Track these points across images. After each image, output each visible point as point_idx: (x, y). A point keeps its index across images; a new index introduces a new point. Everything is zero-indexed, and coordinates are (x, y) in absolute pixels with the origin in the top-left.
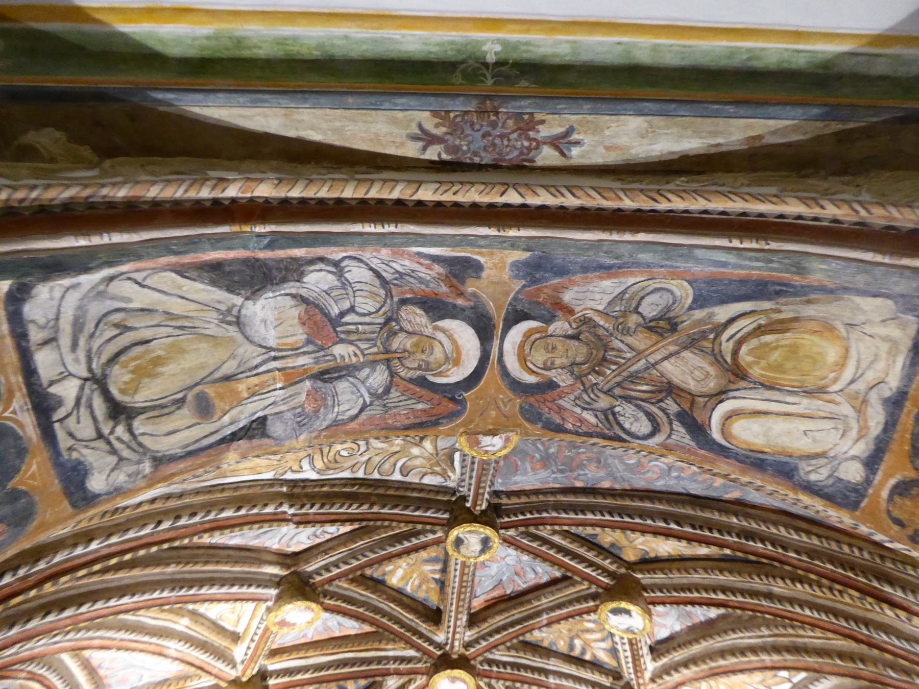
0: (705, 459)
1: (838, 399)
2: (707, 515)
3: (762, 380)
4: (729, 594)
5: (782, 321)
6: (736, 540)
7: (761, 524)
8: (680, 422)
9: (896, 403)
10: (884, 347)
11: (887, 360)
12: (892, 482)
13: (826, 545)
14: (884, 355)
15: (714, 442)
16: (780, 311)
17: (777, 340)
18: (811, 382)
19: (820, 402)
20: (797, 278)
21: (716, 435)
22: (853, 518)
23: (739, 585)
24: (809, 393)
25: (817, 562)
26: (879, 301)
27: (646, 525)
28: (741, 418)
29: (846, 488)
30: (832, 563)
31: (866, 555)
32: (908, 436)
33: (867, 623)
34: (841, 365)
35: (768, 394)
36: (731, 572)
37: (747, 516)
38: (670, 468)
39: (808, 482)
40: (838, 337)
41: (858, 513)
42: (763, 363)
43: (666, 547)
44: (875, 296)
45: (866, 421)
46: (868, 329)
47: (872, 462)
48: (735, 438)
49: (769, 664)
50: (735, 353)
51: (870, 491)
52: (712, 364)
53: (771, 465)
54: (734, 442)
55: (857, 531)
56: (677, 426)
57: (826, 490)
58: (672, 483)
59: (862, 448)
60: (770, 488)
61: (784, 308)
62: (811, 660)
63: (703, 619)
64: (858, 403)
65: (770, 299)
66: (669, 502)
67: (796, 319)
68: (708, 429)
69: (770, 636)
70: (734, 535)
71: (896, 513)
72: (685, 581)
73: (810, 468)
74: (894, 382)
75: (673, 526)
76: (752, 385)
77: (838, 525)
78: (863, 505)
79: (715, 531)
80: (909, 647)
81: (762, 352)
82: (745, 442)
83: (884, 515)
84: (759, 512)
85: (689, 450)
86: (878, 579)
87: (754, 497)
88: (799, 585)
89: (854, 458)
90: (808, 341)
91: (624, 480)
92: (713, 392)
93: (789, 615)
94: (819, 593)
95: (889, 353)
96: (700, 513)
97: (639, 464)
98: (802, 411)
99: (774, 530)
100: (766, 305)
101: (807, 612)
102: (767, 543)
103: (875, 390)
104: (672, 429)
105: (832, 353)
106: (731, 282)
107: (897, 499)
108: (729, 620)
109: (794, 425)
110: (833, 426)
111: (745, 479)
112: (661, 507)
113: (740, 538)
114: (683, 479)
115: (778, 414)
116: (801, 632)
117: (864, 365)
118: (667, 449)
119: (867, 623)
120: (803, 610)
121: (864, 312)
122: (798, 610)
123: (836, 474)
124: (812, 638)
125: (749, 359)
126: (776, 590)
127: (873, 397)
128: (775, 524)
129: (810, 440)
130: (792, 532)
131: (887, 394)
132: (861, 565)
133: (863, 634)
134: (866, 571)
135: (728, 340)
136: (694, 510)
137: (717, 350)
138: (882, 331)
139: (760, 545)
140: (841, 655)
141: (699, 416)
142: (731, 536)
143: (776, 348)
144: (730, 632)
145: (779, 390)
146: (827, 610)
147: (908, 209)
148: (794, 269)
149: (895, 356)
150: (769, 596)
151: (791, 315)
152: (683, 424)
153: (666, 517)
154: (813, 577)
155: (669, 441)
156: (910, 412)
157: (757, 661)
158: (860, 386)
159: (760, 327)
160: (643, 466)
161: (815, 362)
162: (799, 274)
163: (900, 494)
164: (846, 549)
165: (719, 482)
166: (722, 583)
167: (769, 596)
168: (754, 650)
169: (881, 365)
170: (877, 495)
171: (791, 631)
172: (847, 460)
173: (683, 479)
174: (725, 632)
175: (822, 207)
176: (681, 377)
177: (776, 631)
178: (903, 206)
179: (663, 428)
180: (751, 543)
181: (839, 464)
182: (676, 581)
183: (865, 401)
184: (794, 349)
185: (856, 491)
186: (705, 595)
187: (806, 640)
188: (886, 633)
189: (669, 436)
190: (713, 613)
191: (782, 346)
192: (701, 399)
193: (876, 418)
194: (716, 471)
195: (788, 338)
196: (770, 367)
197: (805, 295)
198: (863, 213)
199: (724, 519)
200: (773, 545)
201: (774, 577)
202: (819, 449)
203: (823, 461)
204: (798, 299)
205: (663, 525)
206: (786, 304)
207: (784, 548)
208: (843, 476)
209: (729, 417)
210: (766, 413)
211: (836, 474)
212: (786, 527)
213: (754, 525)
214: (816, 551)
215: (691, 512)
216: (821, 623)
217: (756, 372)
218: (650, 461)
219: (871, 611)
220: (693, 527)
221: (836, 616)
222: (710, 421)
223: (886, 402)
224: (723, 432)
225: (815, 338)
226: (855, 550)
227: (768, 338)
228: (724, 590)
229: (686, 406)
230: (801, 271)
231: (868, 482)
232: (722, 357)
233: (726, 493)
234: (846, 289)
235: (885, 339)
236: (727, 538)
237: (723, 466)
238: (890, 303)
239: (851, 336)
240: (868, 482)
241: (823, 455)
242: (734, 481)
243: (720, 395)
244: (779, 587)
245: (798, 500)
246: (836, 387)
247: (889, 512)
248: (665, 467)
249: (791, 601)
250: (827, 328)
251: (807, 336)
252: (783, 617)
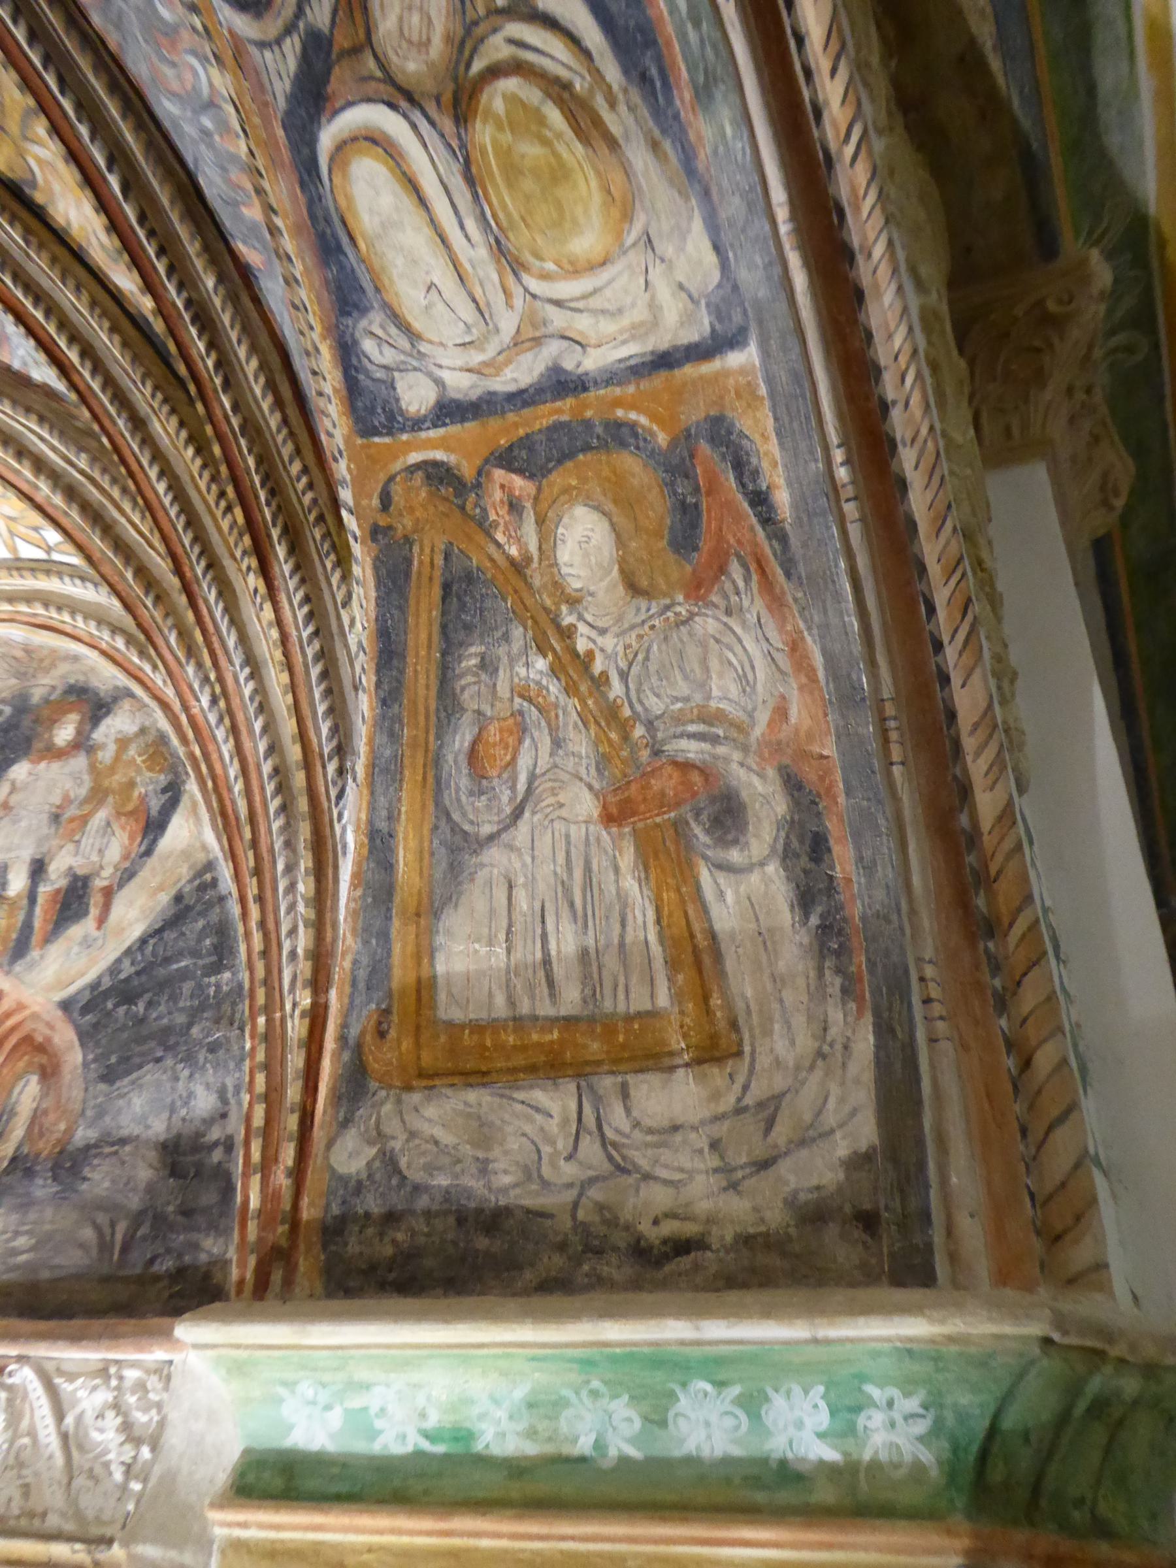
0: (269, 144)
1: (518, 302)
2: (183, 231)
3: (476, 155)
4: (88, 364)
5: (597, 122)
6: (180, 304)
7: (238, 327)
8: (304, 49)
9: (561, 384)
10: (639, 314)
11: (621, 332)
12: (439, 455)
13: (280, 439)
14: (626, 321)
15: (311, 143)
16: (612, 105)
17: (559, 135)
18: (519, 241)
19: (495, 276)
20: (687, 95)
21: (327, 137)
22: (347, 441)
23: (116, 371)
24: (500, 250)
25: (243, 442)
26: (711, 258)
27: (72, 126)
28: (386, 164)
29: (385, 402)
30: (259, 462)
31: (307, 498)
32: (521, 432)
33: (213, 565)
34: (575, 269)
35: (457, 183)
36: (125, 344)
37: (233, 298)
38: (211, 105)
39: (356, 343)
40: (619, 236)
41: (359, 441)
42: (507, 138)
43: (75, 211)
44: (717, 248)
45: (508, 362)
46: (656, 273)
47: (449, 411)
48: (345, 175)
49: (39, 498)
50: (495, 72)
51: (405, 437)
52: (448, 39)
53: (342, 268)
54: (337, 180)
55: (334, 465)
56: (292, 46)
57: (361, 377)
58: (189, 129)
59: (461, 384)
60: (303, 294)
61: (622, 108)
62: (97, 542)
63: (16, 365)
64: (529, 333)
65: (626, 72)
66: (150, 146)
67: (612, 143)
68: (327, 113)
69: (82, 472)
70: (185, 294)
71: (397, 490)
72: (45, 283)
73: (380, 332)
74: (592, 362)
75: (114, 182)
76: (455, 144)
77: (323, 437)
78: (377, 440)
79: (165, 260)
80: (224, 629)
81: (526, 121)
82: (349, 199)
83: (383, 477)
84: (254, 315)
85: (266, 104)
86: (286, 531)
87: (273, 291)
88: (190, 451)
89: (439, 382)
90: (586, 190)
91: (118, 26)
92: (400, 78)
93: (134, 467)
94: (203, 485)
95: (634, 327)
96: (174, 217)
97: (171, 32)
98: (463, 259)
99: (242, 352)
100: (612, 72)
101: (161, 487)
102: (214, 355)
103: (565, 344)
104: (279, 42)
105: (586, 242)
107: (419, 475)
108: (54, 405)
109: (433, 262)
110: (470, 321)
111: (288, 244)
112: (129, 137)
113: (186, 308)
114: (211, 146)
115: (433, 222)
116: (127, 506)
117: (595, 303)
118: (235, 57)
119: (213, 565)
120: (159, 479)
121: (681, 249)
122: (153, 473)
123: (396, 374)
124: (132, 523)
125: (499, 105)
126: (156, 426)
127: (552, 350)
128: (254, 349)
129: (424, 303)
130: (262, 380)
131: (568, 365)
132: (288, 501)
133: (192, 569)
134: (283, 510)
135: (511, 41)
136: (172, 203)
137: (479, 31)
138: (664, 293)
139: (201, 346)
140: (142, 572)
141: (340, 80)
142: (179, 292)
143: (545, 142)
144: (34, 417)
145: (475, 196)
146: (186, 507)
147: (882, 222)
148: (701, 79)
149: (633, 338)
150: (138, 423)
151: (615, 129)
152: (305, 59)
153: (118, 156)
154: (217, 450)
155: (253, 50)
156: (559, 411)
157: (28, 481)
158: (558, 319)
159: (567, 86)
160: (173, 44)
161: (558, 224)
162: (697, 94)
163: (428, 477)
164: (296, 468)
165: (253, 212)
166: (96, 344)
167: (138, 423)
168: (40, 465)
169: (608, 327)
170: (409, 447)
171: (116, 493)
172: (429, 374)
173: (211, 146)
174: (28, 410)
175: (834, 72)
177: (96, 475)
178: (883, 209)
179: (268, 18)
180: (194, 331)
181: (415, 369)
182: (31, 268)
183: (537, 341)
184: (558, 174)
185: (391, 417)
186: (51, 329)
187: (123, 520)
188: (220, 594)
189: (262, 45)
190: (44, 373)
191: (555, 154)
192: (371, 64)
193: (523, 372)
194: (266, 185)
195: (573, 151)
197: (664, 132)
198: (849, 150)
199: (199, 264)
200: (218, 365)
201: (173, 411)
202: (417, 325)
203: (403, 342)
204: (651, 123)
205: (101, 162)
206: (631, 109)
207: (227, 384)
208: (400, 386)
209: (375, 140)
210: (422, 202)
211: (396, 374)
212: (263, 366)
213: (226, 318)
214: (259, 431)
215: (165, 201)
216: (160, 515)
217: (483, 134)
218: (195, 53)
219: (235, 559)
220: (142, 219)
221: (188, 524)
222: (343, 108)
224: (342, 147)
225: (597, 198)
226: (304, 480)
227: (554, 116)
228: (88, 352)
229: (342, 41)
230: (704, 94)
231: (417, 424)
232: (474, 50)
233: (245, 242)
234: (706, 193)
235: (654, 307)
236: (172, 289)
237: (282, 189)
238: (716, 276)
239: (631, 254)
240: (417, 424)
241: (413, 335)
242: (273, 231)
243: (402, 96)
244: (164, 428)
245: (317, 350)
246: (534, 285)
247: (391, 479)
248: (205, 90)
249: (158, 456)
250: (623, 206)
251: (594, 183)
252: (123, 461)
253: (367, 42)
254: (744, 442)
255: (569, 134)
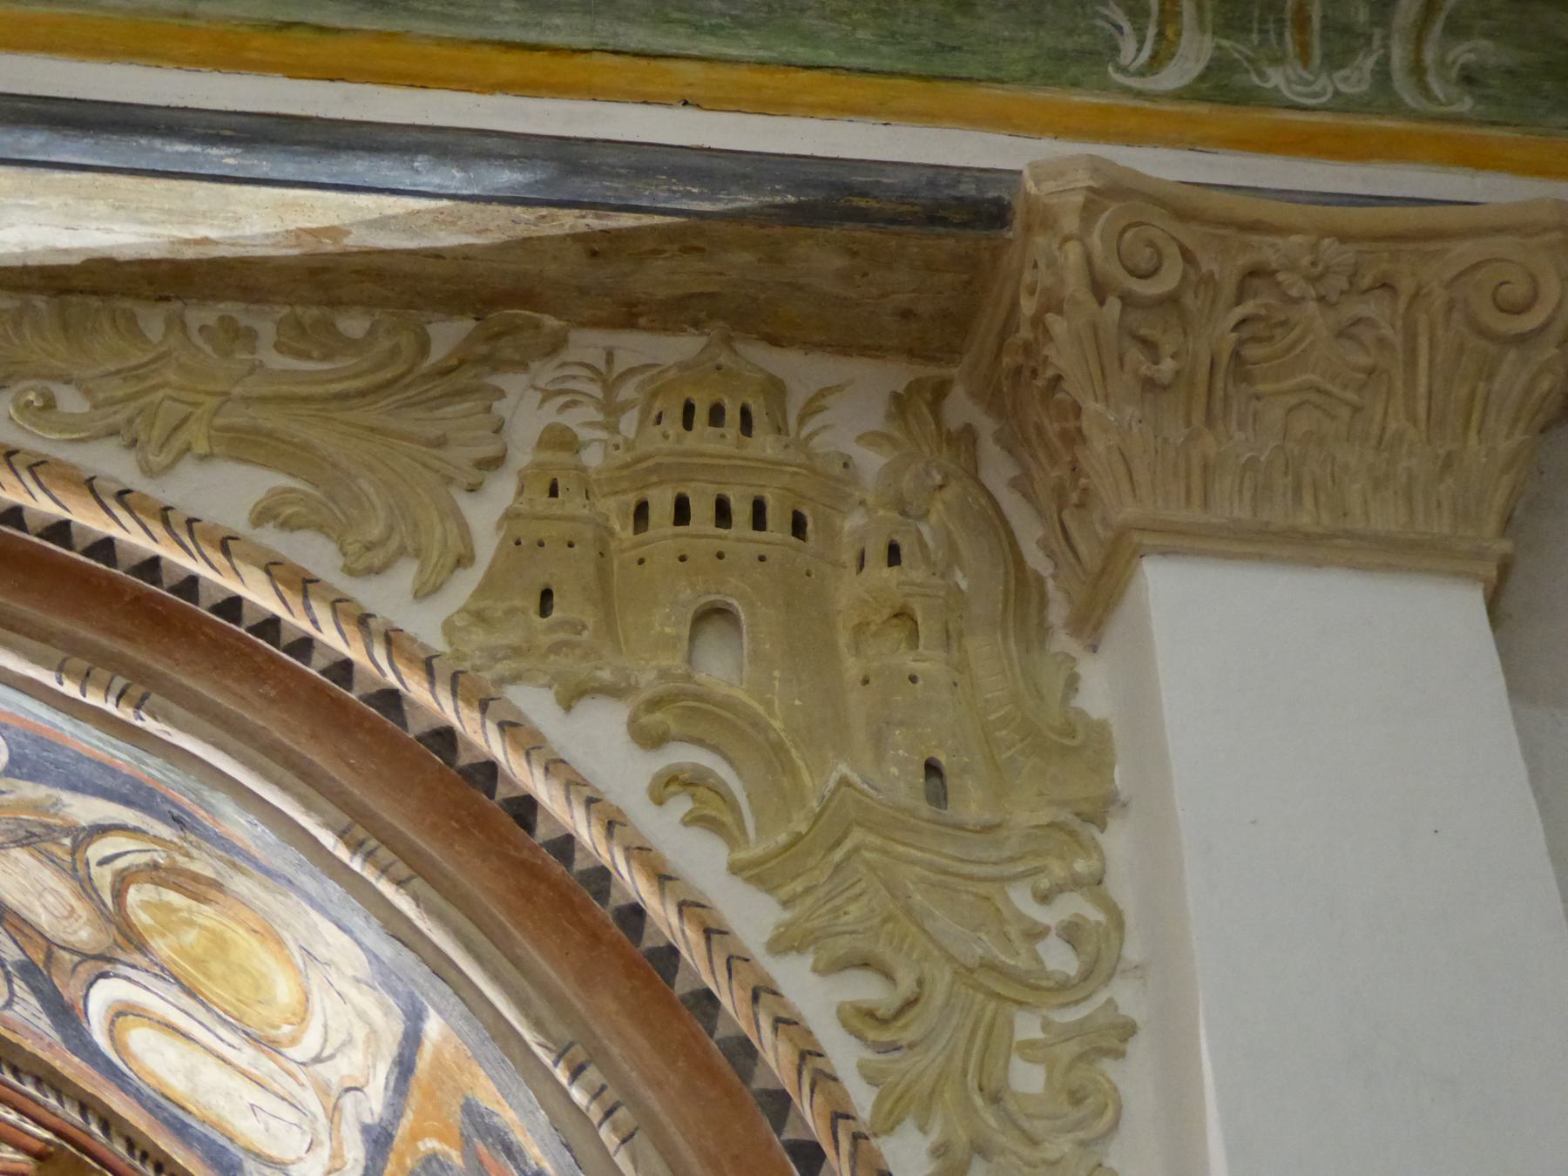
1: (302, 1078)
3: (175, 970)
5: (196, 878)
8: (27, 983)
24: (256, 1041)
28: (143, 1025)
35: (186, 1001)
42: (171, 939)
46: (334, 978)
48: (135, 1058)
50: (119, 894)
68: (83, 1020)
104: (12, 993)
105: (284, 990)
106: (80, 758)
110: (296, 1121)
129: (262, 1127)
143: (191, 923)
145: (203, 1004)
147: (477, 715)
176: (20, 897)
178: (468, 702)
184: (220, 943)
192: (66, 956)
195: (206, 914)
196: (183, 952)
202: (274, 1152)
209: (121, 1012)
210: (186, 1036)
217: (161, 946)
222: (85, 1005)
223: (366, 1130)
243: (101, 963)
250: (269, 934)
251: (241, 931)
253: (50, 946)
254: (495, 1119)
255: (194, 903)
